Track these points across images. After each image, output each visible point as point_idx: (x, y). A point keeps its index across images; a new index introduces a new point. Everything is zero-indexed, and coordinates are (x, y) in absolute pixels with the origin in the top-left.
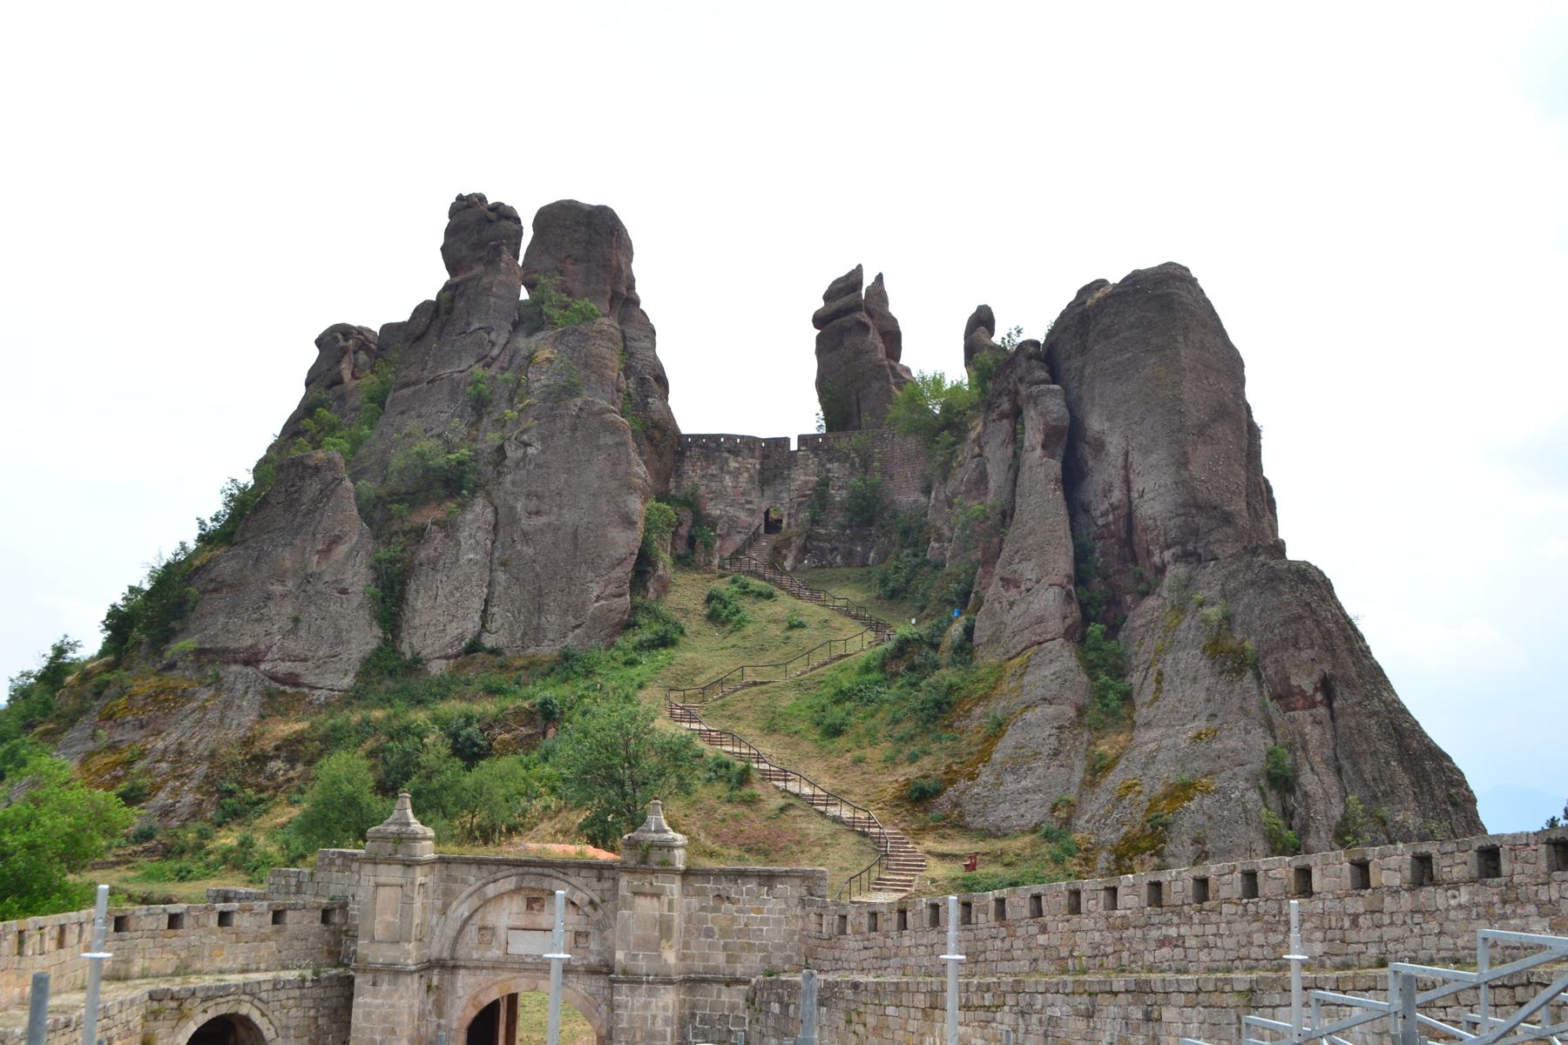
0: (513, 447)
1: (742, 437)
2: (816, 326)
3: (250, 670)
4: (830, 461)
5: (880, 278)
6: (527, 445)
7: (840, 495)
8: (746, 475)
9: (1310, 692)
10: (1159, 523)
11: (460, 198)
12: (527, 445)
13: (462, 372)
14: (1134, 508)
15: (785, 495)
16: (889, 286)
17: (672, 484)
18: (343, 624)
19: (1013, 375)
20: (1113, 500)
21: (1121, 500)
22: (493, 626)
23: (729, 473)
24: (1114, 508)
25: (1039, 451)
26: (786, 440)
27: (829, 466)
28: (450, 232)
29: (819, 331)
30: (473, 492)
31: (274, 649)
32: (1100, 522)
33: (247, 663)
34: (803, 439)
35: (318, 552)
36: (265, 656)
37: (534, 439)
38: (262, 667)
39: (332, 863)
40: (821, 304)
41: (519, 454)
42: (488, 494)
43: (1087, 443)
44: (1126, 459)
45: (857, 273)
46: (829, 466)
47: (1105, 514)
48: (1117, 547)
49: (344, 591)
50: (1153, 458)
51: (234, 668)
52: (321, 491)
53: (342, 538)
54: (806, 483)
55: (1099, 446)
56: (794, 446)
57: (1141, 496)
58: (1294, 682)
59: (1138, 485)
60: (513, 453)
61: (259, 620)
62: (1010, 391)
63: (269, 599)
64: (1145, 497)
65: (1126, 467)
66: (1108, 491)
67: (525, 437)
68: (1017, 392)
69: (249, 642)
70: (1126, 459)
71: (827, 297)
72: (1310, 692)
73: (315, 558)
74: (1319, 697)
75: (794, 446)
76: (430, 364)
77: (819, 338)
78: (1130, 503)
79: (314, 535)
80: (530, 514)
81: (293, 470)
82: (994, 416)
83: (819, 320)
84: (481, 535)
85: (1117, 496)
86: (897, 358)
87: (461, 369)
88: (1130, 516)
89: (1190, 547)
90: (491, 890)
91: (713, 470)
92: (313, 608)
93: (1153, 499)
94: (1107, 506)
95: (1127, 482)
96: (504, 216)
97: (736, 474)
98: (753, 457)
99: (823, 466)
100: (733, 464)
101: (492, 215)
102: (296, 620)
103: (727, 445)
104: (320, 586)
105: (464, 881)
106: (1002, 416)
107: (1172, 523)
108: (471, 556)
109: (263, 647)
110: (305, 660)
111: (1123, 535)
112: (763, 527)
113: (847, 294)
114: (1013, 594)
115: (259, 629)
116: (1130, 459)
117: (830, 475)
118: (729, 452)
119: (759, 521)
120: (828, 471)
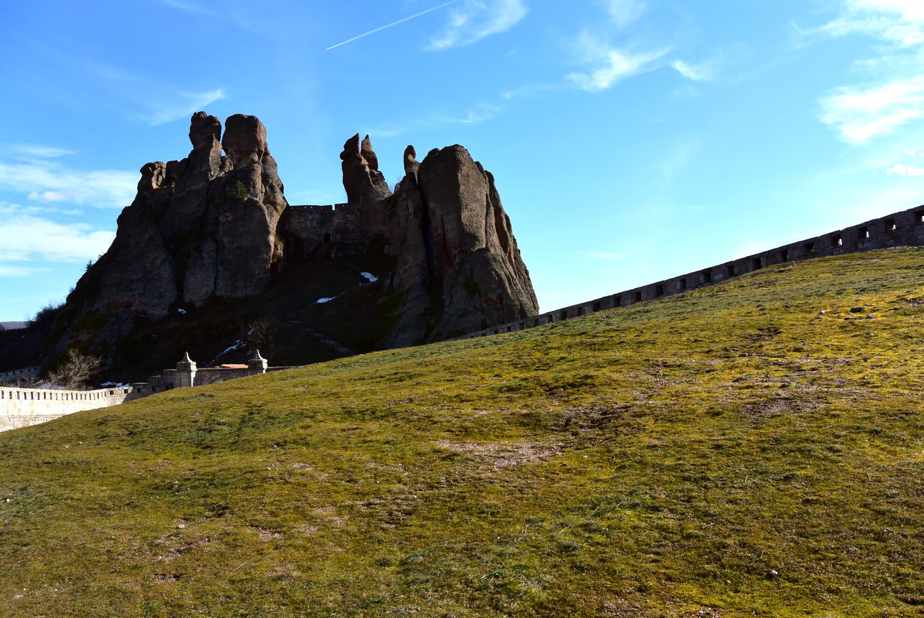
1: (313, 206)
2: (342, 158)
5: (367, 137)
6: (227, 217)
8: (315, 221)
9: (495, 298)
12: (227, 217)
15: (331, 228)
16: (371, 140)
17: (286, 226)
18: (162, 290)
20: (439, 232)
22: (219, 287)
23: (308, 220)
24: (439, 235)
25: (413, 216)
26: (331, 206)
28: (191, 128)
31: (136, 301)
32: (436, 240)
33: (126, 307)
34: (336, 206)
38: (132, 308)
39: (167, 373)
40: (343, 149)
41: (224, 220)
44: (442, 218)
45: (356, 138)
47: (437, 237)
49: (161, 277)
51: (122, 309)
54: (339, 223)
55: (434, 213)
56: (334, 209)
58: (490, 296)
59: (446, 228)
65: (442, 220)
66: (437, 228)
67: (226, 214)
70: (442, 218)
72: (495, 298)
73: (149, 265)
74: (498, 301)
75: (334, 209)
76: (188, 184)
77: (342, 163)
82: (401, 199)
83: (342, 156)
86: (376, 168)
88: (444, 238)
89: (463, 249)
90: (213, 378)
91: (302, 220)
97: (311, 221)
98: (318, 213)
100: (310, 217)
102: (144, 289)
105: (205, 376)
108: (208, 261)
109: (132, 301)
112: (323, 241)
118: (308, 212)
119: (322, 238)
120: (347, 218)
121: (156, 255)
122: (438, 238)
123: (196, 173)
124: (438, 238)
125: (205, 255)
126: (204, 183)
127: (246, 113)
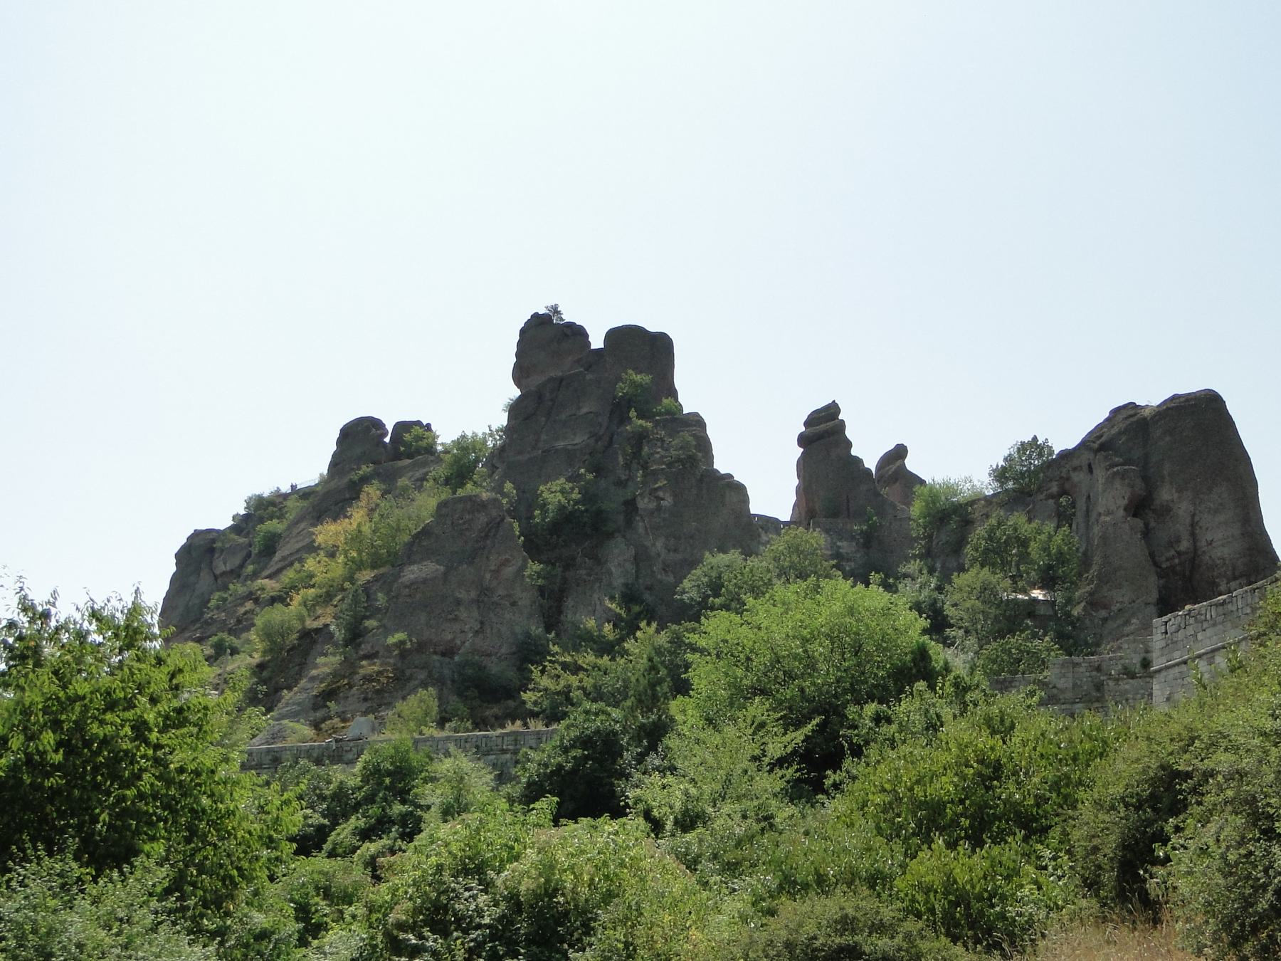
0: (646, 500)
3: (447, 660)
4: (840, 540)
7: (850, 566)
10: (1227, 562)
11: (536, 316)
13: (574, 445)
14: (1199, 553)
19: (1067, 466)
21: (1188, 549)
24: (1179, 554)
25: (1121, 512)
27: (839, 544)
29: (802, 450)
30: (610, 535)
31: (467, 644)
32: (1164, 566)
33: (443, 654)
35: (490, 571)
36: (459, 650)
37: (667, 495)
40: (803, 429)
41: (653, 505)
42: (624, 536)
43: (1154, 511)
46: (839, 544)
48: (1180, 583)
49: (514, 604)
50: (1221, 518)
51: (435, 657)
52: (488, 524)
53: (510, 562)
55: (1166, 511)
57: (1211, 544)
60: (644, 504)
61: (456, 619)
62: (1061, 478)
63: (459, 604)
64: (1214, 545)
67: (661, 494)
68: (1068, 479)
69: (450, 637)
71: (806, 424)
73: (488, 576)
76: (544, 437)
78: (1196, 549)
79: (488, 558)
80: (669, 551)
81: (460, 506)
83: (803, 440)
84: (630, 566)
85: (1185, 545)
87: (575, 442)
88: (1194, 558)
92: (492, 615)
93: (1223, 546)
94: (1172, 552)
95: (1193, 535)
96: (576, 333)
99: (835, 543)
101: (568, 332)
102: (482, 623)
103: (760, 523)
104: (495, 599)
106: (1052, 496)
107: (1239, 562)
109: (458, 642)
110: (489, 655)
111: (1187, 573)
113: (827, 422)
114: (1103, 613)
115: (457, 627)
116: (1197, 519)
117: (841, 550)
120: (839, 547)
121: (507, 557)
122: (1177, 561)
123: (563, 417)
124: (1177, 561)
125: (612, 568)
126: (586, 438)
127: (652, 327)
